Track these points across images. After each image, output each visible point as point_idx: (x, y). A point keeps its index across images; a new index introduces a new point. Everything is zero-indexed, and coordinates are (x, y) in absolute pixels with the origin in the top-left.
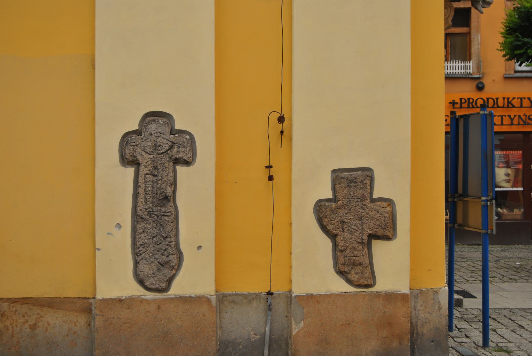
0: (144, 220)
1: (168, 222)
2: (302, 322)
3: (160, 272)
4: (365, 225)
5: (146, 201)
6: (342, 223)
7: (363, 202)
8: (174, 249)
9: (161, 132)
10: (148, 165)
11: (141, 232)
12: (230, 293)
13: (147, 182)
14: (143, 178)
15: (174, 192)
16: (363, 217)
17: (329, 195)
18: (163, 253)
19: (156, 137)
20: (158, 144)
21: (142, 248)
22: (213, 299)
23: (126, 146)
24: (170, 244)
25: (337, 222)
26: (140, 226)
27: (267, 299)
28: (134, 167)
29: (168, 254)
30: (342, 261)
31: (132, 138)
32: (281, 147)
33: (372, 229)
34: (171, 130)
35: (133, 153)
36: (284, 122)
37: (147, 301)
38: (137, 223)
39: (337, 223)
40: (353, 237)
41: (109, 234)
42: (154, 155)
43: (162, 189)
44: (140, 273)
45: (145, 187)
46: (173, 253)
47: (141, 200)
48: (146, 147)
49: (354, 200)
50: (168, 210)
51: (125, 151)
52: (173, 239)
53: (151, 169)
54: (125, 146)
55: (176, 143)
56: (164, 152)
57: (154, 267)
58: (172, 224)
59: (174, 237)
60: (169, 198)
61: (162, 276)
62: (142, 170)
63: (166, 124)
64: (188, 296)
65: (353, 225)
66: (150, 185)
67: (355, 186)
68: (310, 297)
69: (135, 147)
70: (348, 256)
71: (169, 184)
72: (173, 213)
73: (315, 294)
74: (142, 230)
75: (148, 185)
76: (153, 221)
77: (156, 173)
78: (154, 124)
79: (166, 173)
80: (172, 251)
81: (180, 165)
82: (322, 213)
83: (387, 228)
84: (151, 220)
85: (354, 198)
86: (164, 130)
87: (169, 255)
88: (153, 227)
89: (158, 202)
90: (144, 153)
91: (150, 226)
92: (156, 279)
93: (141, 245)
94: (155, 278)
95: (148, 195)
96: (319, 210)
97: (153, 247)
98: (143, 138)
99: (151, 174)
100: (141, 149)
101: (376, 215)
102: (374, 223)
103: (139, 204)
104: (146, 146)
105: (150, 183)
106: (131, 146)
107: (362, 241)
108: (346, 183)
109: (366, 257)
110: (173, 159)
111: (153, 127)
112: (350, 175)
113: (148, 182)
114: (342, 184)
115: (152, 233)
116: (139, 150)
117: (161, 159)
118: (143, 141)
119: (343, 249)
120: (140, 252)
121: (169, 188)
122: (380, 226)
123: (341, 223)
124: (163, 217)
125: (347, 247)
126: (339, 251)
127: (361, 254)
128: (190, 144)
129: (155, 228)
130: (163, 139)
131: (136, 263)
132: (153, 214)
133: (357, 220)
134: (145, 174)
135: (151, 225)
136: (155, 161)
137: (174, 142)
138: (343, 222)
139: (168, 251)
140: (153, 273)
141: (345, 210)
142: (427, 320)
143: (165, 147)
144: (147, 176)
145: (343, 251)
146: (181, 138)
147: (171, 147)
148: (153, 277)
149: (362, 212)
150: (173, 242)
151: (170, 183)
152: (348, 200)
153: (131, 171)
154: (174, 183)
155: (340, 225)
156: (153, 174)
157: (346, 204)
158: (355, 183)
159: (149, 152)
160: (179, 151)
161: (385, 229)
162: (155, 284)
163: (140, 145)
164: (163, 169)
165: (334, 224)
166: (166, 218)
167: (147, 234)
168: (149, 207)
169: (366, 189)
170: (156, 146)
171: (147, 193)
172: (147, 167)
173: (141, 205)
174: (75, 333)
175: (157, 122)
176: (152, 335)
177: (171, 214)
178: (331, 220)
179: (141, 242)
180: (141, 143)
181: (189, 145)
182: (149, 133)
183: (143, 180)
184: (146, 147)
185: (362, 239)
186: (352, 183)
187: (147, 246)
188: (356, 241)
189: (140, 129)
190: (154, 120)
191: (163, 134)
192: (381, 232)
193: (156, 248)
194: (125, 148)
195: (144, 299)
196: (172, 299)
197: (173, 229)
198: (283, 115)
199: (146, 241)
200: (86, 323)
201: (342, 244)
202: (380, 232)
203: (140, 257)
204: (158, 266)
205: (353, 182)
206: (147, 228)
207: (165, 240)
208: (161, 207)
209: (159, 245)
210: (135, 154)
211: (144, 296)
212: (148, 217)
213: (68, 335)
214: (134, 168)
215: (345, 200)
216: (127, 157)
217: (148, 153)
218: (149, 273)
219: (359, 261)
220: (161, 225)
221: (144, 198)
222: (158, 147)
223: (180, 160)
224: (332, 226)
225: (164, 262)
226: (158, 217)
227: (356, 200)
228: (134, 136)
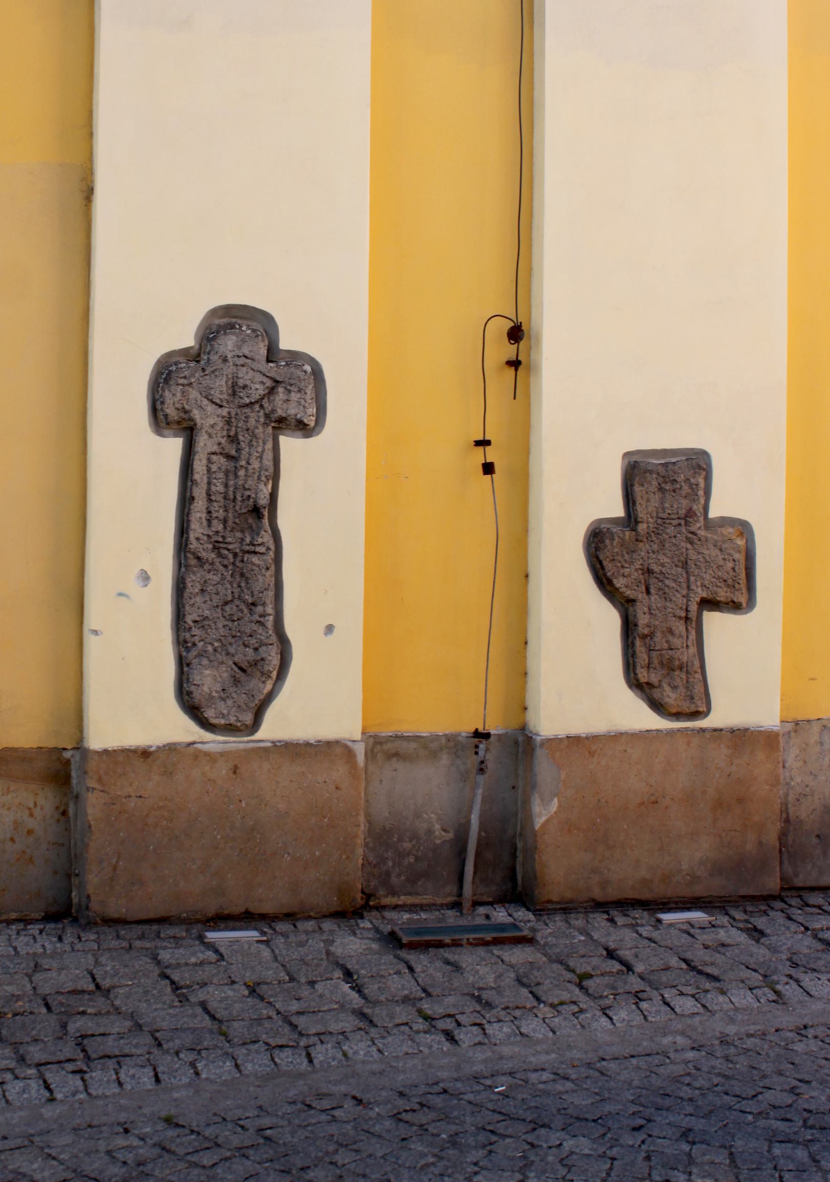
1: (257, 569)
2: (556, 800)
3: (239, 685)
4: (692, 579)
8: (271, 632)
10: (215, 432)
11: (197, 590)
12: (390, 734)
13: (213, 472)
14: (204, 462)
15: (274, 496)
17: (617, 510)
18: (246, 643)
19: (237, 365)
20: (241, 383)
21: (199, 628)
22: (360, 751)
23: (166, 386)
25: (636, 570)
26: (194, 578)
27: (477, 747)
29: (256, 645)
30: (644, 660)
31: (179, 366)
32: (515, 398)
34: (269, 350)
36: (521, 339)
37: (207, 754)
38: (187, 570)
40: (668, 604)
41: (120, 594)
42: (229, 408)
44: (193, 688)
45: (209, 483)
46: (270, 642)
47: (198, 515)
50: (260, 540)
51: (161, 396)
52: (270, 609)
53: (223, 441)
56: (253, 401)
57: (225, 675)
58: (268, 574)
59: (271, 603)
61: (244, 696)
62: (202, 444)
64: (302, 742)
65: (668, 578)
68: (574, 741)
70: (656, 648)
73: (584, 735)
74: (199, 587)
75: (216, 479)
76: (226, 566)
77: (233, 453)
78: (232, 334)
79: (257, 452)
80: (267, 637)
81: (286, 432)
83: (737, 586)
84: (220, 562)
86: (255, 349)
87: (260, 647)
88: (223, 578)
89: (237, 520)
91: (216, 578)
92: (230, 702)
93: (195, 622)
94: (228, 701)
95: (215, 504)
96: (597, 544)
97: (224, 626)
98: (205, 368)
99: (221, 454)
100: (201, 394)
105: (221, 475)
107: (687, 614)
108: (655, 483)
109: (693, 650)
113: (215, 472)
115: (221, 594)
116: (194, 394)
118: (206, 375)
119: (646, 632)
121: (262, 486)
122: (725, 581)
124: (246, 556)
127: (683, 643)
130: (251, 372)
131: (183, 665)
133: (676, 566)
134: (209, 454)
135: (220, 576)
137: (278, 379)
138: (649, 571)
139: (258, 636)
140: (223, 690)
142: (808, 789)
143: (257, 389)
144: (214, 458)
145: (646, 636)
146: (292, 370)
147: (272, 391)
148: (223, 699)
149: (687, 549)
150: (270, 615)
152: (659, 521)
153: (174, 445)
156: (226, 454)
157: (654, 530)
159: (218, 401)
162: (228, 714)
163: (198, 384)
165: (629, 575)
166: (255, 559)
168: (217, 532)
169: (696, 497)
170: (235, 389)
172: (214, 436)
173: (197, 529)
174: (30, 832)
175: (237, 331)
176: (219, 837)
178: (623, 567)
179: (195, 615)
181: (311, 387)
183: (205, 468)
185: (687, 610)
187: (209, 625)
190: (232, 326)
191: (253, 359)
192: (726, 594)
193: (230, 629)
194: (163, 391)
195: (200, 751)
196: (265, 749)
197: (269, 585)
198: (521, 323)
199: (207, 613)
200: (57, 808)
201: (646, 621)
202: (723, 594)
203: (194, 652)
204: (235, 672)
206: (210, 582)
207: (250, 609)
208: (242, 531)
209: (236, 623)
211: (199, 743)
212: (213, 555)
213: (12, 840)
216: (168, 411)
217: (216, 404)
218: (215, 688)
219: (679, 660)
220: (242, 575)
221: (205, 511)
222: (241, 390)
224: (625, 579)
226: (235, 555)
228: (184, 363)
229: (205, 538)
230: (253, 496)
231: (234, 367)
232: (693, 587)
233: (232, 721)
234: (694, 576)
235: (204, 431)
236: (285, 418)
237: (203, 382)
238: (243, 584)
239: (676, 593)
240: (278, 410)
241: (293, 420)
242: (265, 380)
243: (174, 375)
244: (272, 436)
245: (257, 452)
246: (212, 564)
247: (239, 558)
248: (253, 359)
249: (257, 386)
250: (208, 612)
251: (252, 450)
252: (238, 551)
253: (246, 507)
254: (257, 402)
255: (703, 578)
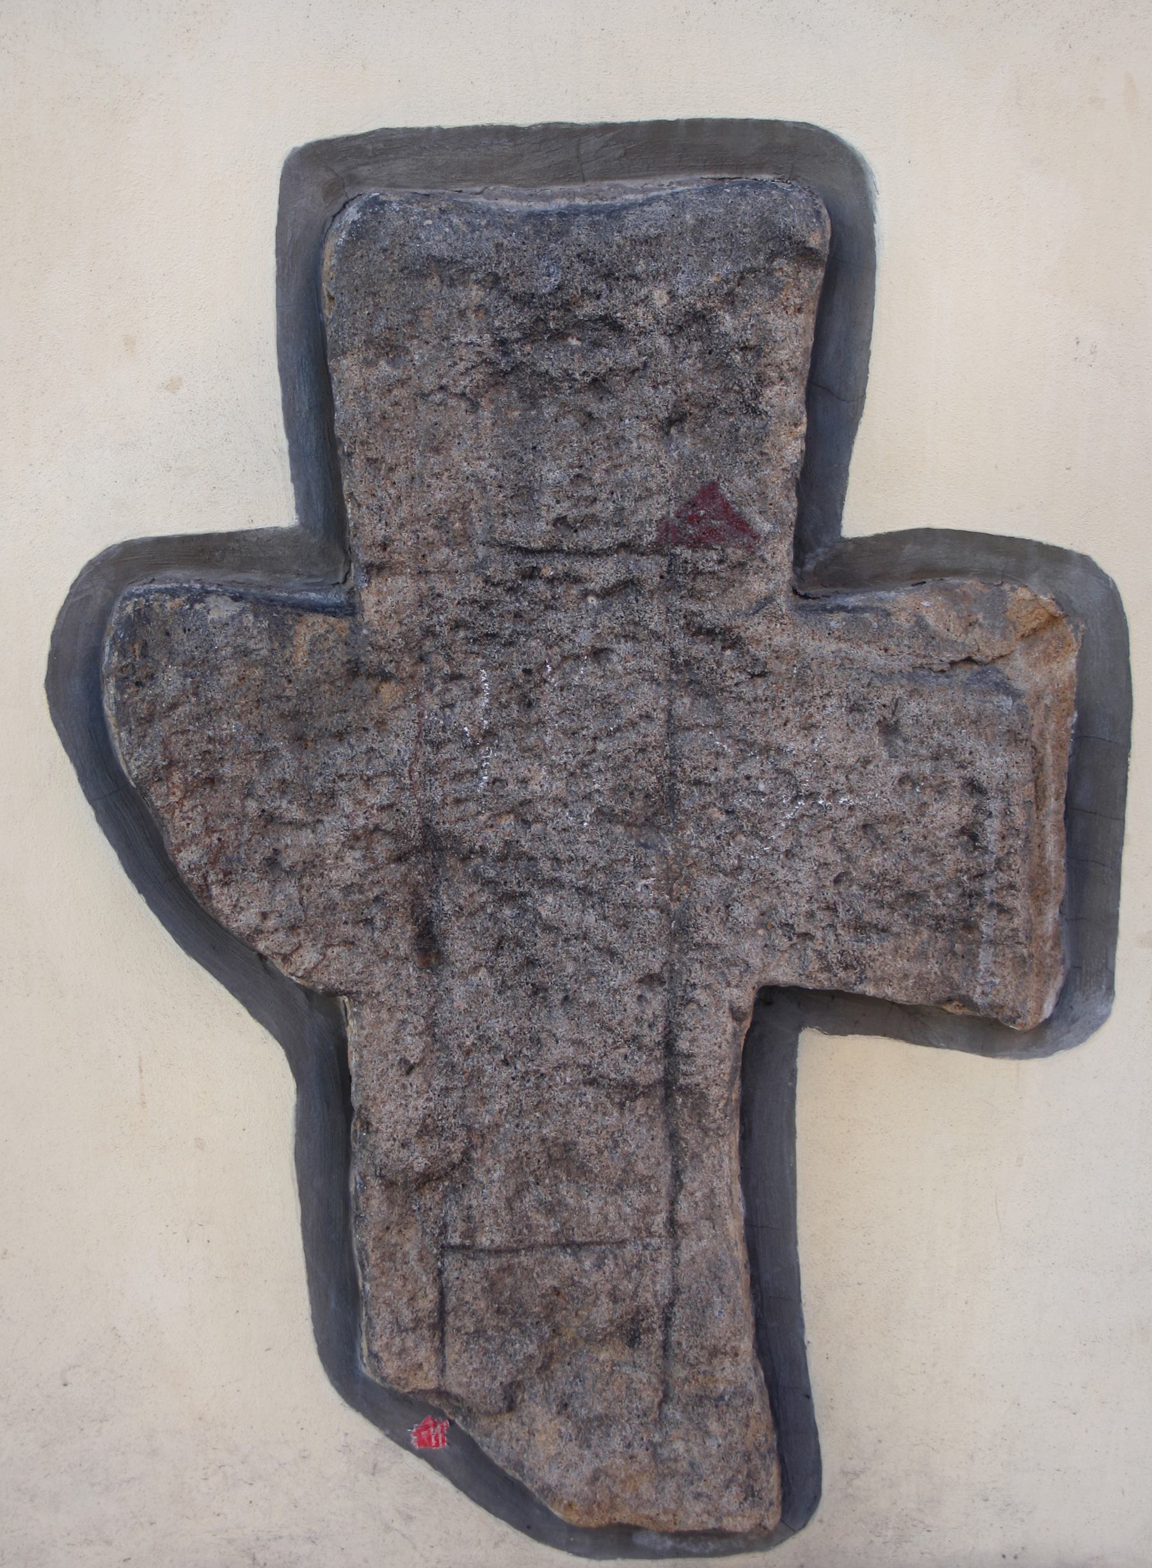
6: (421, 850)
7: (693, 594)
16: (698, 782)
33: (807, 936)
39: (350, 857)
49: (582, 567)
65: (555, 884)
67: (598, 385)
70: (484, 1240)
82: (149, 719)
85: (583, 537)
101: (866, 762)
102: (833, 857)
112: (542, 216)
114: (418, 354)
122: (912, 896)
123: (400, 859)
125: (476, 1137)
126: (375, 1182)
141: (455, 690)
155: (395, 872)
157: (464, 614)
158: (596, 344)
161: (969, 926)
165: (312, 865)
169: (747, 424)
186: (559, 336)
188: (588, 1068)
205: (579, 325)
215: (460, 563)
224: (291, 888)
227: (605, 572)
232: (709, 929)
234: (715, 870)
239: (599, 964)
255: (764, 882)
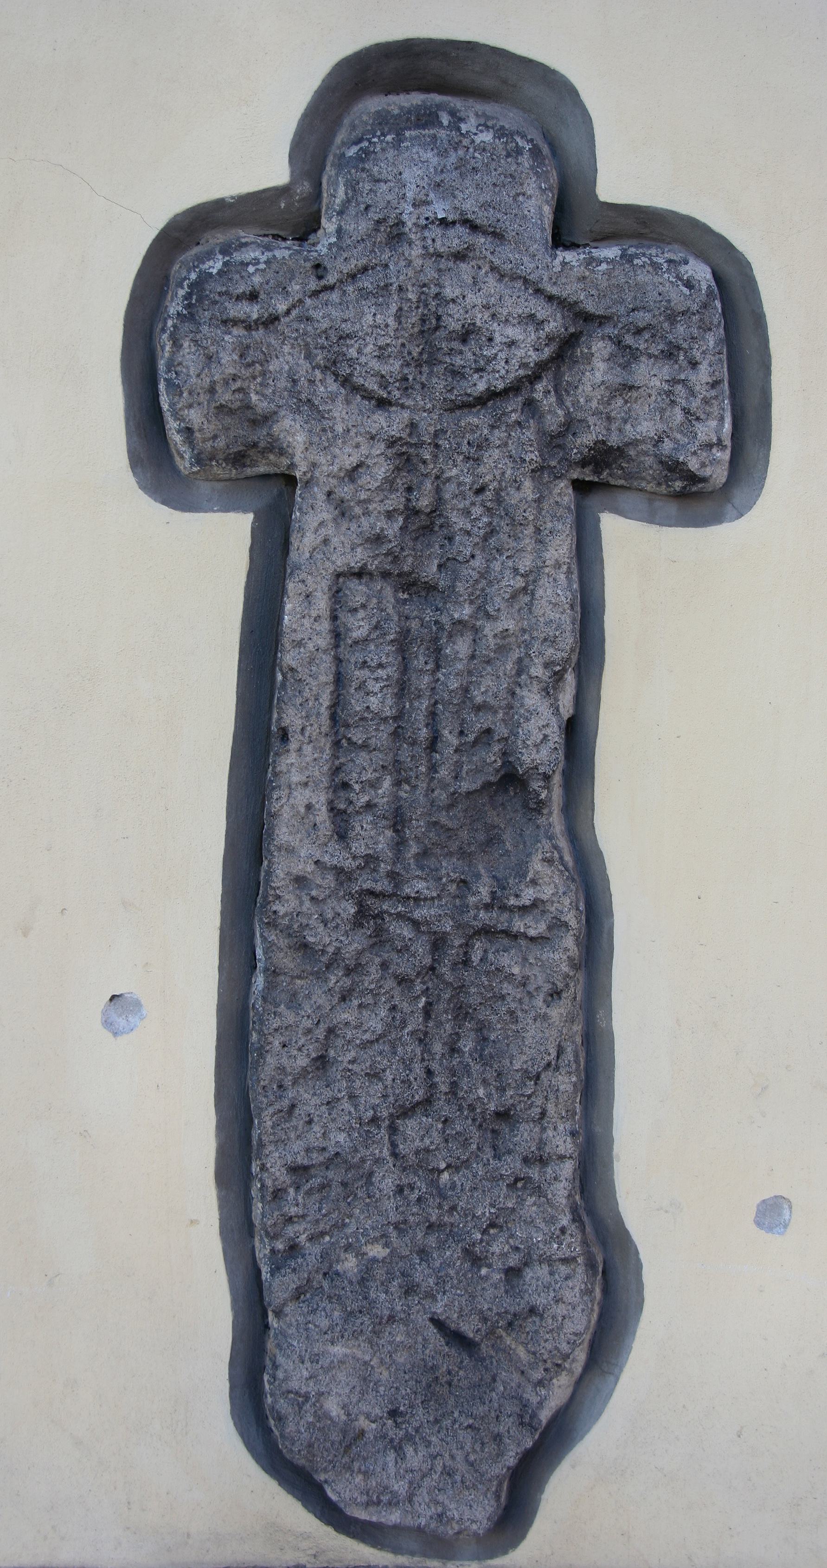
0: (328, 967)
1: (518, 993)
5: (342, 806)
9: (481, 218)
13: (356, 643)
14: (322, 604)
19: (439, 255)
24: (534, 1173)
28: (245, 511)
29: (513, 1260)
31: (238, 256)
34: (562, 210)
35: (238, 384)
42: (414, 409)
43: (479, 708)
45: (339, 680)
47: (301, 797)
48: (349, 336)
53: (392, 529)
54: (175, 326)
55: (602, 320)
56: (500, 386)
58: (556, 1013)
60: (536, 785)
63: (519, 151)
66: (381, 673)
69: (259, 334)
71: (537, 670)
72: (571, 918)
76: (403, 981)
77: (430, 571)
78: (424, 146)
89: (443, 818)
90: (333, 387)
91: (375, 1023)
92: (415, 1458)
93: (298, 1171)
94: (409, 1450)
95: (362, 758)
99: (386, 575)
100: (308, 356)
103: (283, 834)
104: (347, 328)
106: (225, 322)
110: (575, 455)
111: (412, 176)
117: (480, 447)
118: (331, 288)
120: (290, 1231)
124: (478, 945)
128: (722, 331)
129: (412, 1033)
132: (399, 916)
134: (338, 575)
136: (424, 462)
137: (590, 307)
140: (394, 1413)
143: (512, 344)
150: (562, 1158)
151: (546, 665)
154: (574, 658)
159: (372, 385)
160: (631, 388)
164: (492, 541)
167: (349, 1079)
171: (358, 736)
172: (358, 510)
175: (442, 134)
177: (550, 928)
180: (308, 301)
182: (379, 222)
183: (325, 625)
184: (349, 336)
189: (305, 188)
191: (498, 236)
194: (177, 344)
210: (254, 397)
214: (251, 516)
217: (368, 396)
221: (325, 782)
222: (456, 345)
223: (630, 460)
225: (485, 1320)
226: (438, 943)
229: (330, 880)
230: (502, 731)
231: (429, 263)
233: (423, 1521)
235: (319, 493)
236: (620, 452)
237: (317, 314)
238: (467, 1045)
240: (591, 420)
241: (649, 461)
242: (542, 310)
243: (214, 288)
244: (570, 519)
245: (516, 570)
246: (354, 969)
247: (453, 953)
248: (498, 236)
249: (513, 332)
250: (342, 1137)
251: (496, 566)
252: (448, 926)
253: (478, 771)
254: (513, 389)
